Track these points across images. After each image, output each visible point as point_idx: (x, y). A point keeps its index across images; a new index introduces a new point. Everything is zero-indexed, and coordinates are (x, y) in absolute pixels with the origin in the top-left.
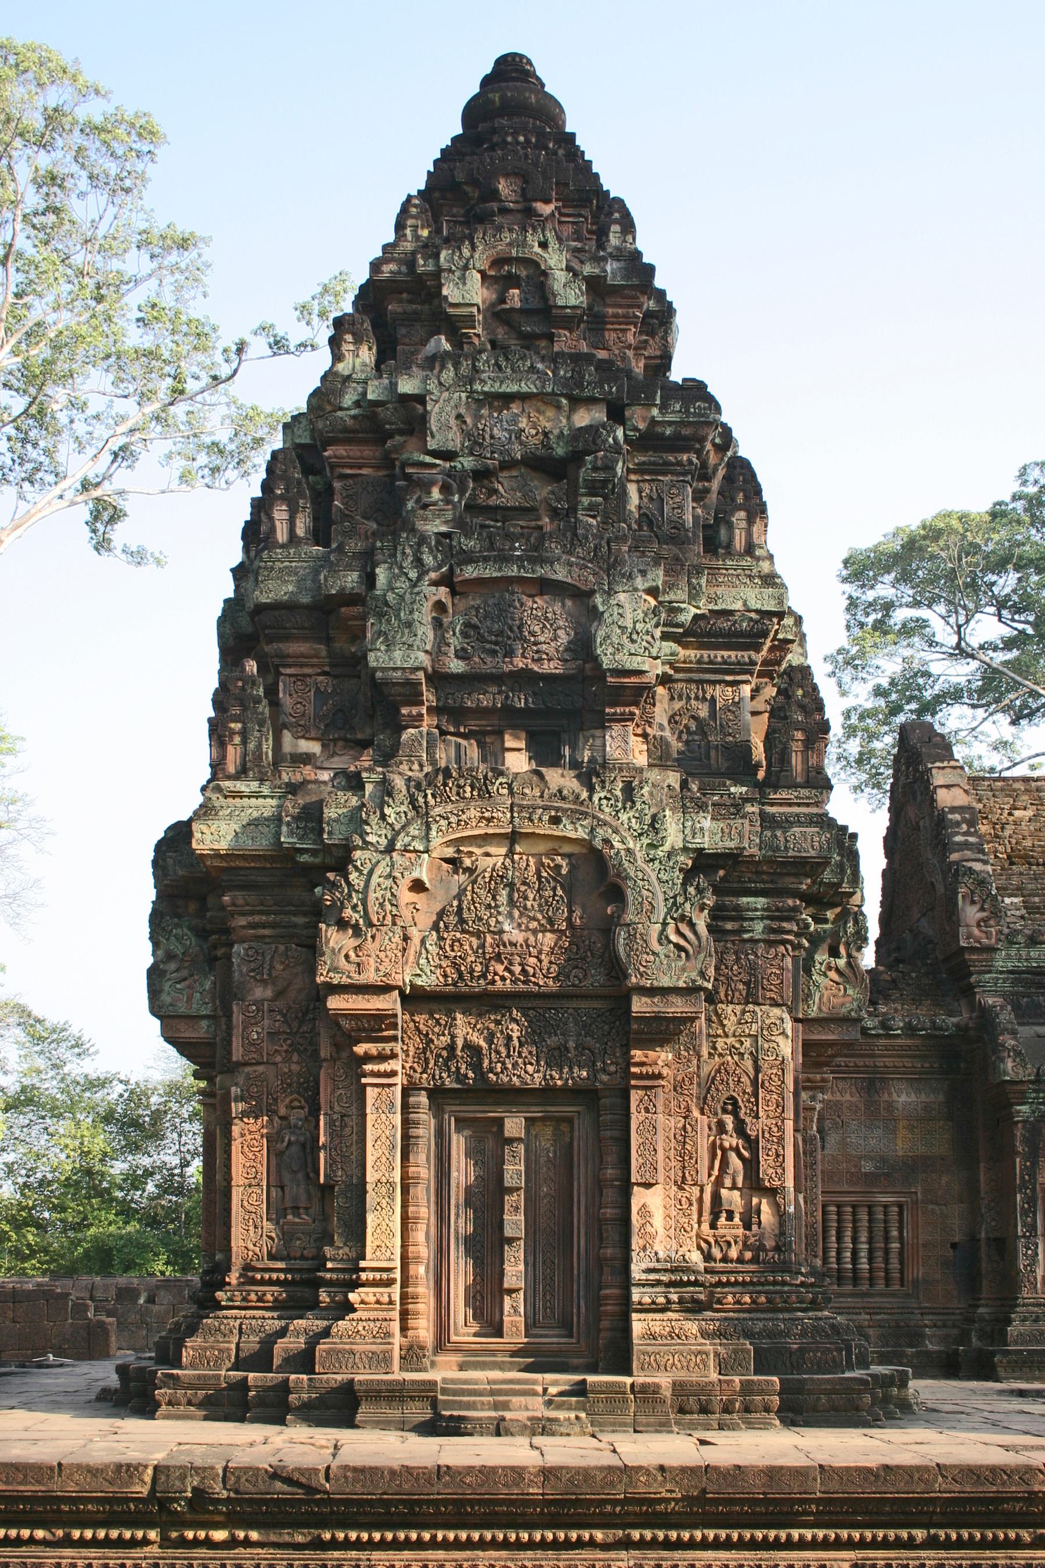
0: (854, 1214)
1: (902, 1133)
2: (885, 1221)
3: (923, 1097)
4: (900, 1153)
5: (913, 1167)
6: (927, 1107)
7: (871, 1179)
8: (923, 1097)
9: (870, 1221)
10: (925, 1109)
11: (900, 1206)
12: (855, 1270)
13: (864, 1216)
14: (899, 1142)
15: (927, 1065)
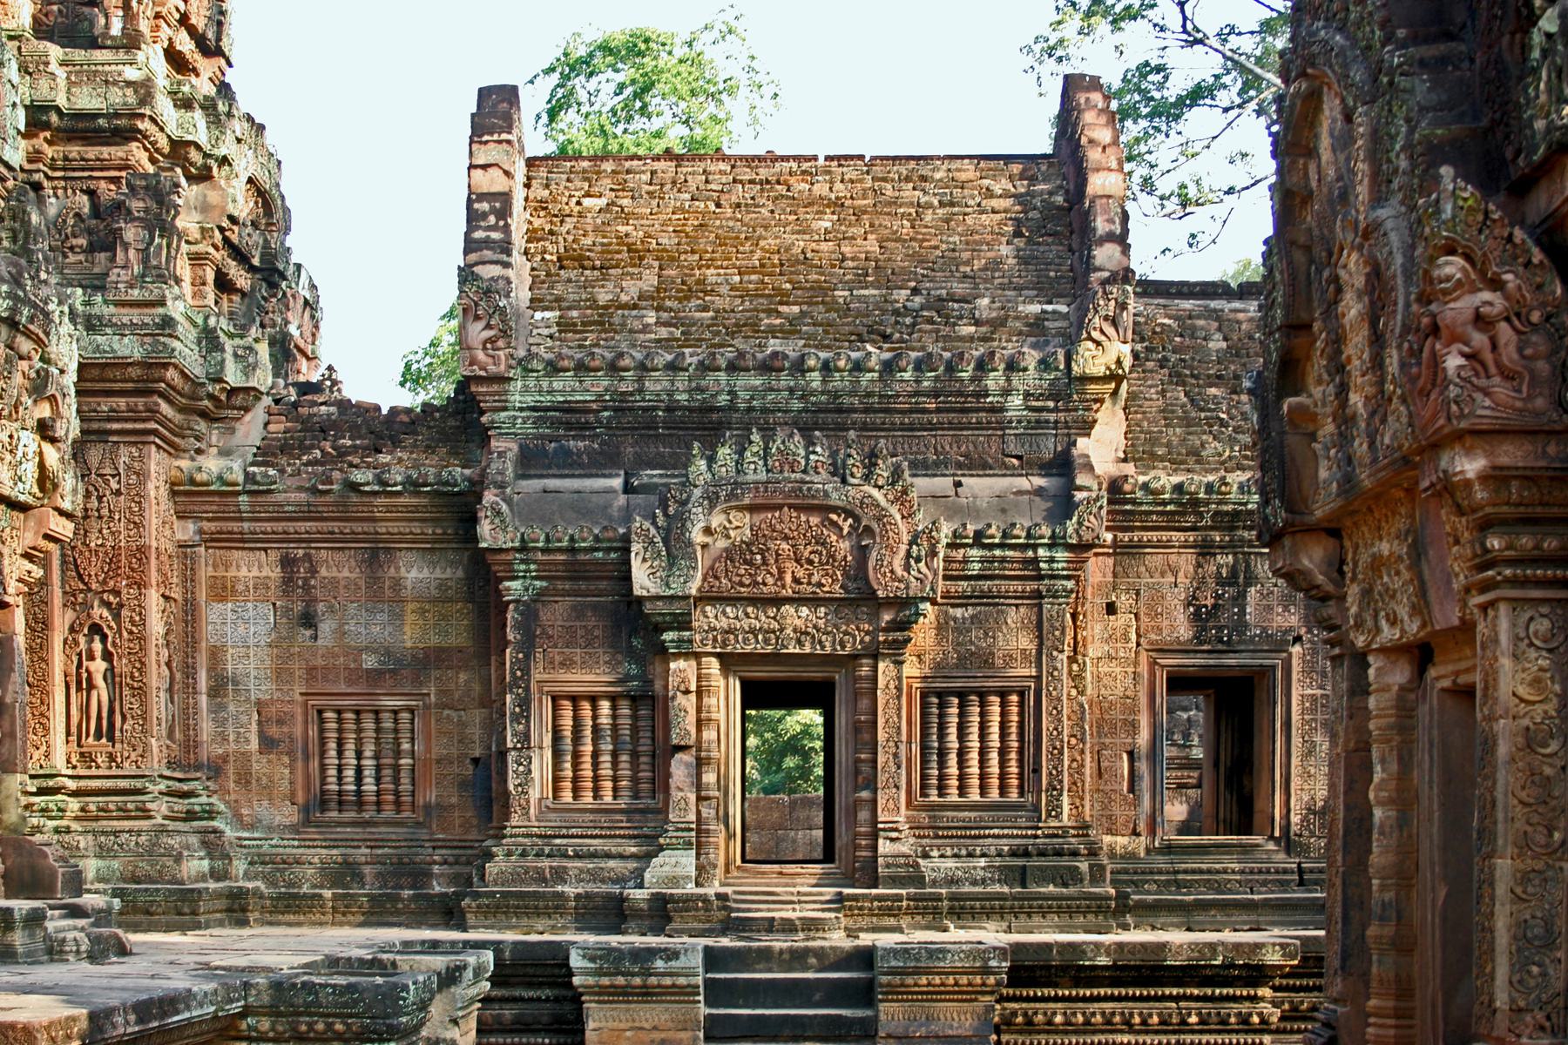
0: (358, 721)
1: (410, 618)
2: (396, 731)
3: (438, 573)
4: (409, 644)
5: (428, 661)
6: (442, 585)
7: (375, 676)
8: (438, 573)
9: (378, 730)
10: (439, 587)
11: (411, 711)
12: (359, 793)
13: (369, 724)
14: (407, 629)
15: (439, 531)
